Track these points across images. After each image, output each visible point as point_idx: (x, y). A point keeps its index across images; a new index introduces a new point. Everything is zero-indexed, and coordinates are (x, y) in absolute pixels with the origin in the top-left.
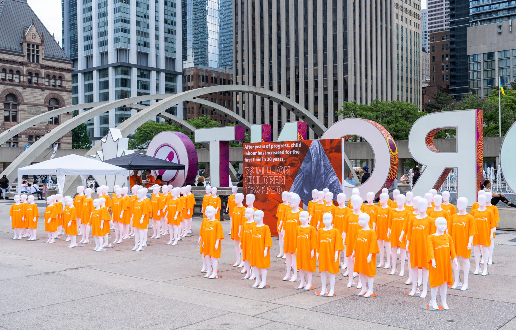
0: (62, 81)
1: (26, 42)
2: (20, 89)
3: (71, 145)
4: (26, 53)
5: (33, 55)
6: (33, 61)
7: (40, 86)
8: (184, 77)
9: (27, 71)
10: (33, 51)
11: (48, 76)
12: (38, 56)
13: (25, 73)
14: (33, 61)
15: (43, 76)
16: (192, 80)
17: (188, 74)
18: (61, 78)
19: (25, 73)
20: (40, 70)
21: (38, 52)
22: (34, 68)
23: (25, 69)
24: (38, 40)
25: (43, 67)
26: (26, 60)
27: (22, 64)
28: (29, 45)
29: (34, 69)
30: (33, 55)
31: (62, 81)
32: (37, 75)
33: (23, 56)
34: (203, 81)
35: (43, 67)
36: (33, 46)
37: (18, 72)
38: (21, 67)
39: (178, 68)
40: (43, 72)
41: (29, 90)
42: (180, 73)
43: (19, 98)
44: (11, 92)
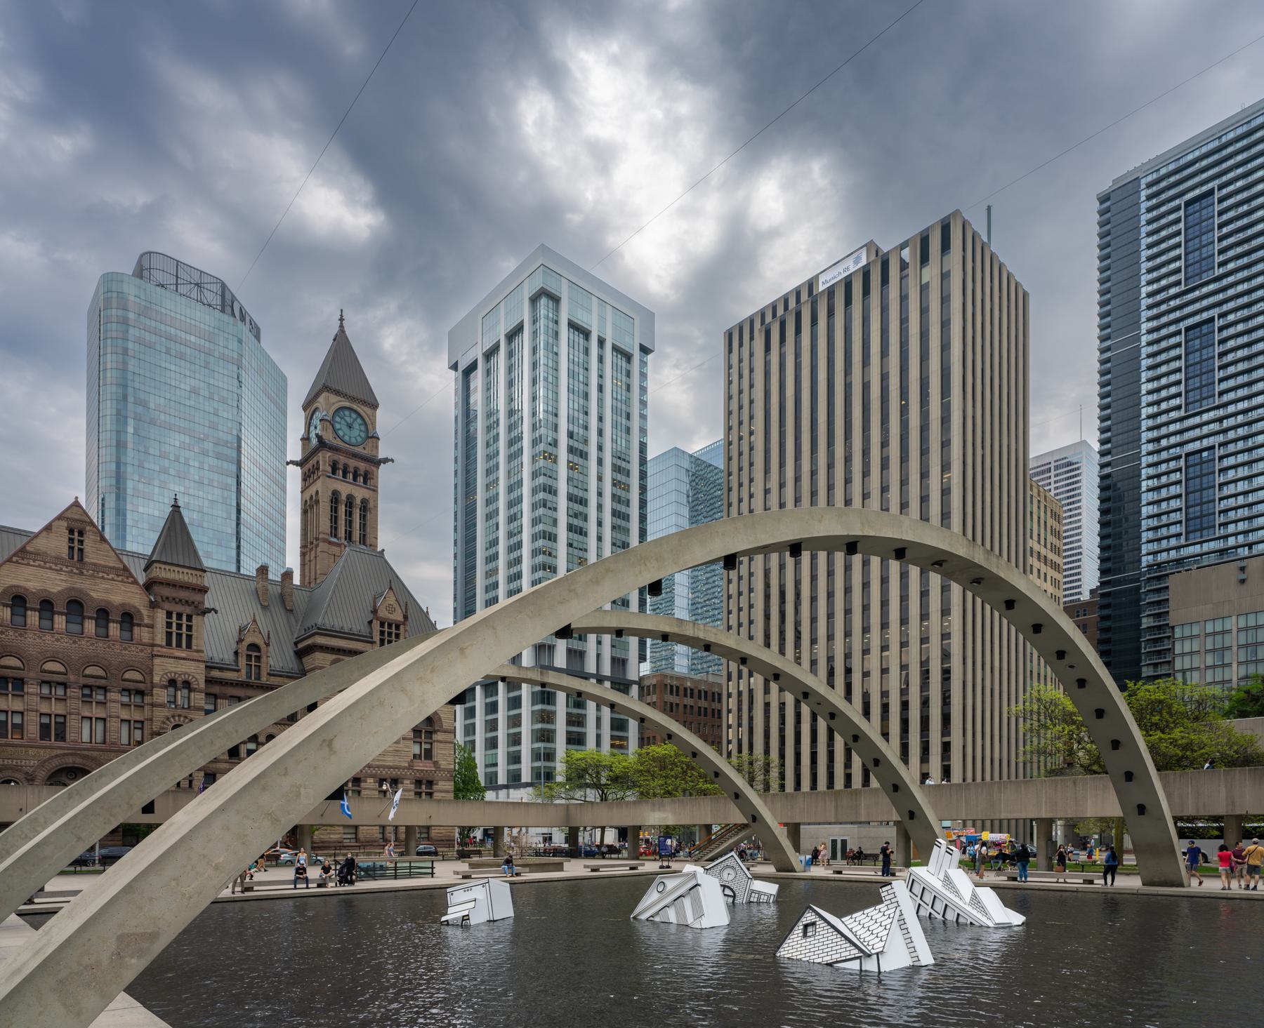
8: (641, 688)
16: (654, 692)
17: (646, 683)
34: (671, 693)
39: (632, 675)
42: (635, 682)
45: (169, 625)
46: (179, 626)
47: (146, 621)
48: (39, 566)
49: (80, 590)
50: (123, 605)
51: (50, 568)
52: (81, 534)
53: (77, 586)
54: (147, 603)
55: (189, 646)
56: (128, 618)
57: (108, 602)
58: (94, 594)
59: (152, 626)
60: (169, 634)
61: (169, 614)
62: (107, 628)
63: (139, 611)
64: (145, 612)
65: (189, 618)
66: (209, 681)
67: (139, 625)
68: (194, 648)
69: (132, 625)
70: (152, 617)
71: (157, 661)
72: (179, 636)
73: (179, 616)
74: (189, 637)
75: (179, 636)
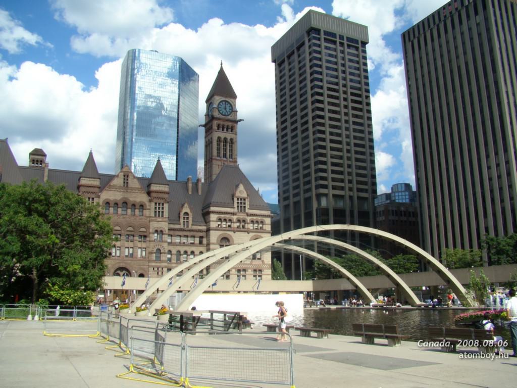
0: (263, 225)
1: (236, 197)
2: (231, 233)
3: (270, 276)
4: (236, 205)
5: (241, 207)
6: (241, 211)
7: (246, 230)
9: (237, 219)
10: (241, 203)
11: (252, 222)
12: (245, 207)
13: (235, 221)
14: (241, 211)
15: (249, 222)
18: (262, 222)
19: (235, 221)
20: (247, 217)
21: (245, 203)
22: (242, 216)
23: (235, 218)
24: (245, 195)
25: (248, 215)
26: (236, 210)
27: (233, 214)
28: (238, 199)
29: (242, 217)
30: (241, 207)
31: (263, 225)
32: (244, 221)
33: (234, 208)
35: (248, 215)
36: (241, 199)
37: (230, 220)
38: (232, 216)
40: (249, 219)
41: (237, 233)
43: (231, 240)
44: (225, 236)
45: (156, 208)
46: (159, 208)
47: (148, 207)
48: (115, 191)
49: (126, 198)
50: (140, 202)
51: (117, 191)
52: (128, 176)
53: (126, 196)
54: (148, 200)
55: (163, 216)
56: (142, 206)
57: (135, 202)
58: (131, 199)
59: (149, 209)
60: (156, 212)
61: (156, 204)
62: (134, 211)
63: (145, 204)
64: (147, 204)
65: (163, 204)
66: (170, 229)
67: (145, 209)
68: (164, 216)
69: (143, 209)
70: (150, 206)
71: (151, 223)
72: (159, 212)
73: (159, 204)
74: (163, 212)
75: (159, 212)
